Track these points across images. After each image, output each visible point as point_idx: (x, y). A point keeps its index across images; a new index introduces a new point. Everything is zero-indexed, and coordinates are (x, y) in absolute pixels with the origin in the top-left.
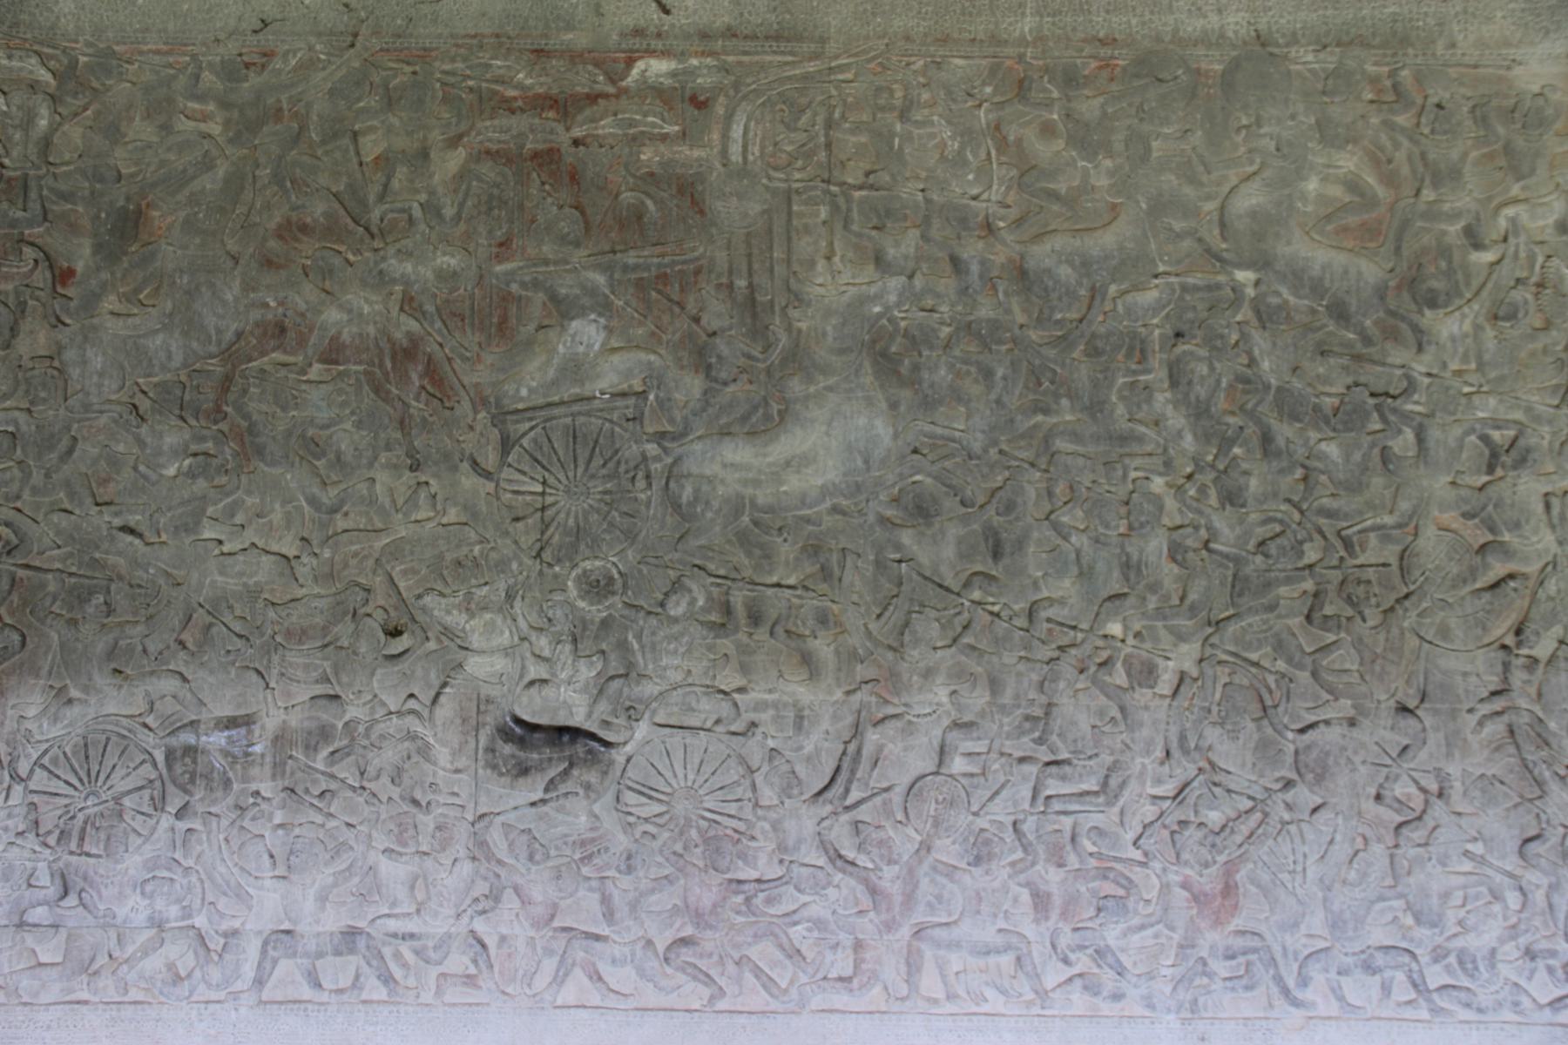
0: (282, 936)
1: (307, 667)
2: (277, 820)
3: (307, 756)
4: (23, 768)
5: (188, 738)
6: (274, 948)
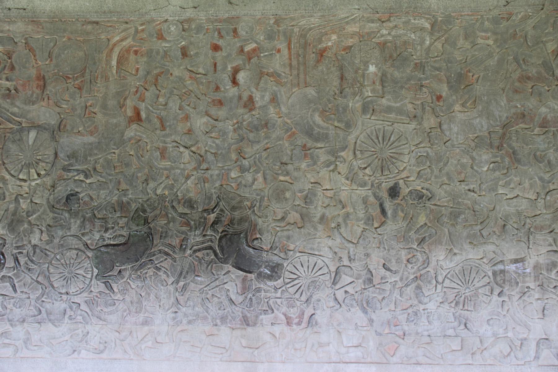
0: (545, 341)
1: (544, 240)
2: (537, 297)
3: (548, 273)
4: (440, 279)
5: (500, 267)
6: (543, 345)
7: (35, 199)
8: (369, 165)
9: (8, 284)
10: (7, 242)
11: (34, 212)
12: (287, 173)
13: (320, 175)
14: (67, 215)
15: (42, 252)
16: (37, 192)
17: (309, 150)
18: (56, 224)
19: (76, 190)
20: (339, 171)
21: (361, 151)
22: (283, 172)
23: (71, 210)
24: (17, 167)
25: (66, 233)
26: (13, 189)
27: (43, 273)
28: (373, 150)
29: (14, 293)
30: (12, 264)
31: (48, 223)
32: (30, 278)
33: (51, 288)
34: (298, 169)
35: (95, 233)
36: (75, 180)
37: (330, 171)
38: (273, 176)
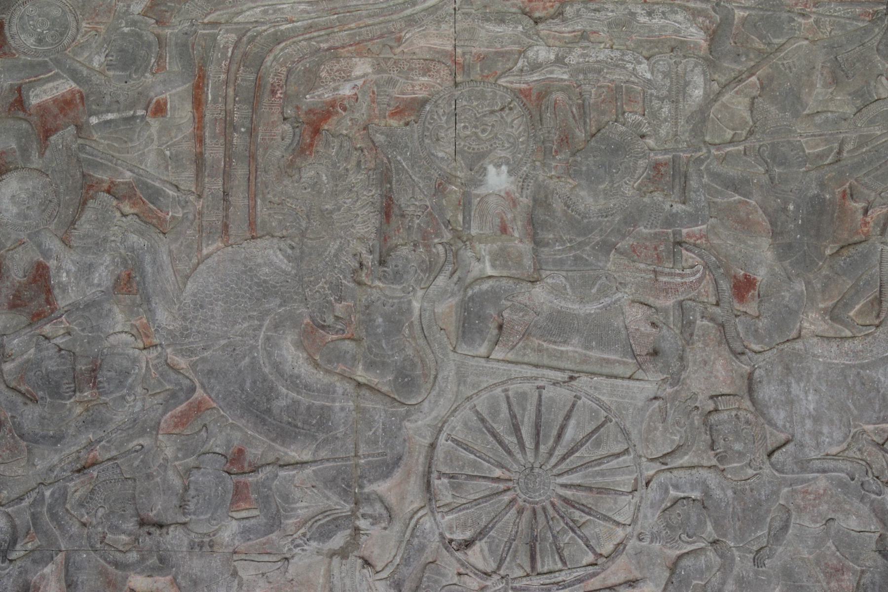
8: (482, 534)
12: (161, 560)
13: (292, 570)
17: (255, 470)
20: (366, 554)
21: (452, 477)
22: (143, 559)
28: (498, 473)
34: (205, 546)
37: (332, 554)
38: (103, 573)
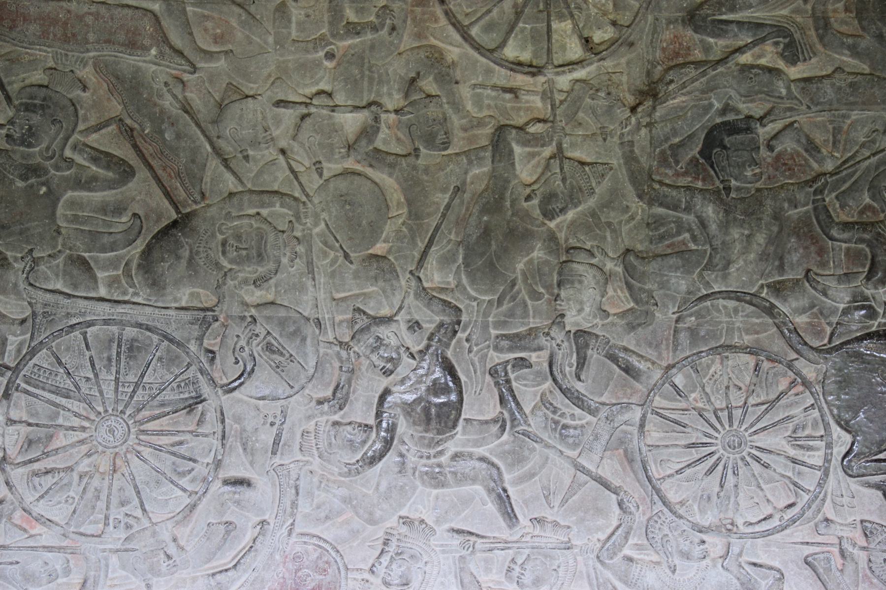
7: (573, 145)
9: (479, 488)
10: (464, 318)
11: (573, 199)
14: (710, 211)
15: (613, 358)
16: (581, 114)
18: (660, 248)
19: (745, 108)
23: (728, 189)
24: (495, 11)
25: (708, 285)
26: (478, 101)
27: (621, 442)
29: (501, 522)
30: (492, 409)
31: (627, 243)
32: (567, 465)
33: (659, 506)
35: (832, 283)
36: (745, 69)
